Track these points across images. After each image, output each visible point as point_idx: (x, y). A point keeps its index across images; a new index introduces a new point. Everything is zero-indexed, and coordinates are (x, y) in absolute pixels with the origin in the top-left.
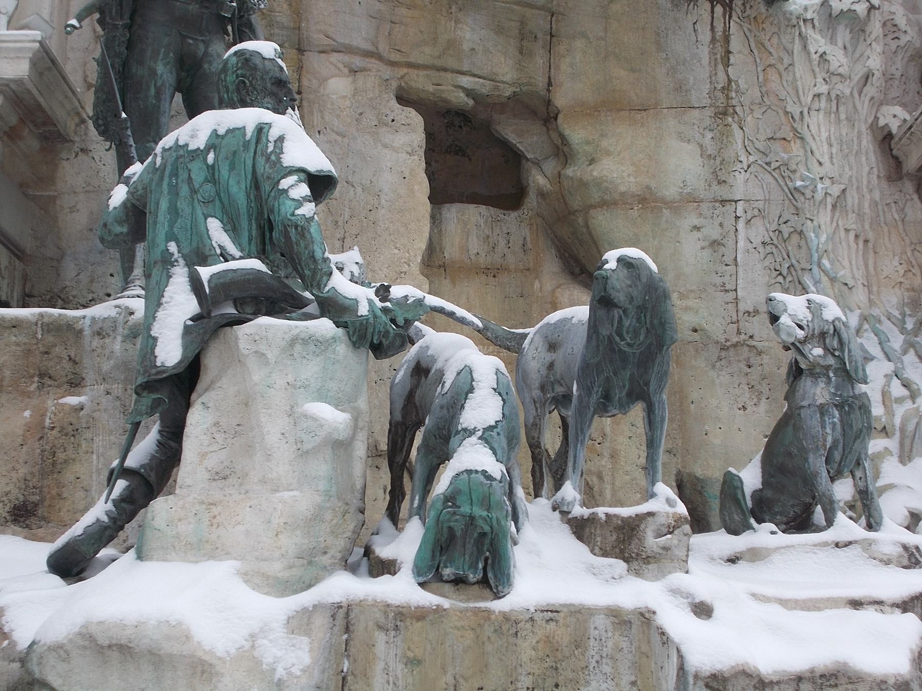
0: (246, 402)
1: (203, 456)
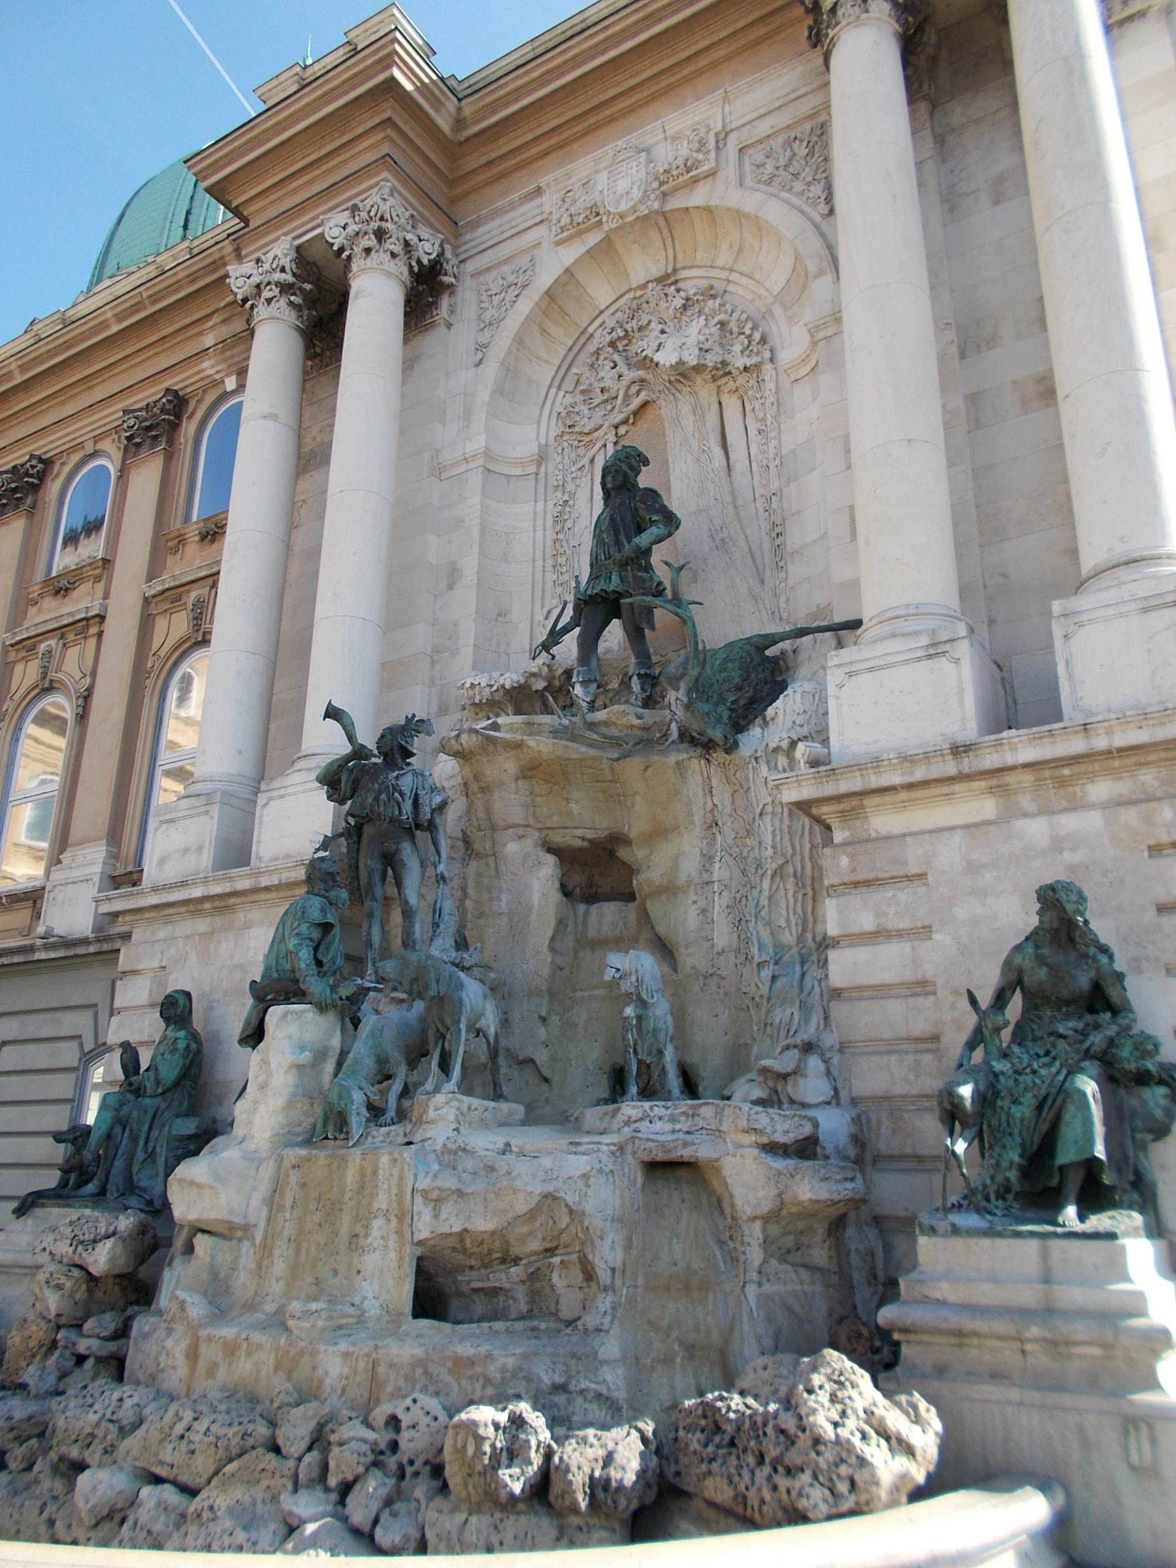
1: (257, 1077)
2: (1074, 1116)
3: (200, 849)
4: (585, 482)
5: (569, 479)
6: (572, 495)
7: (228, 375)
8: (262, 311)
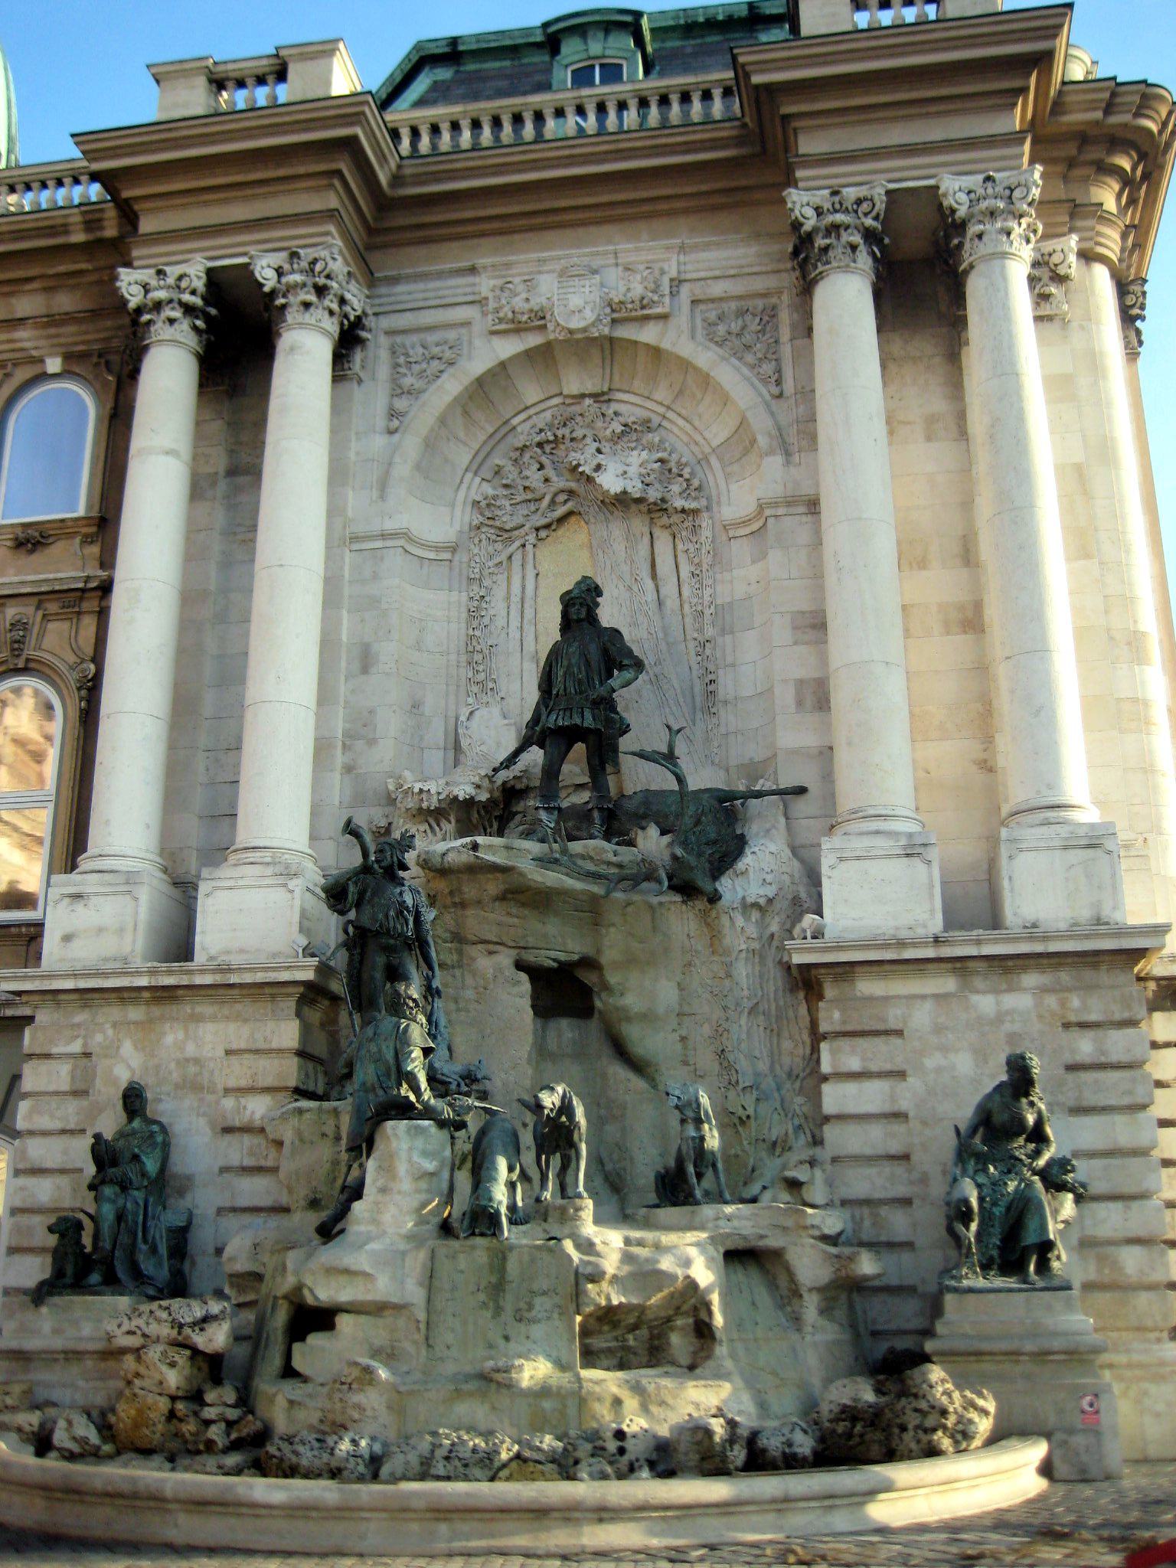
0: (391, 1156)
1: (374, 1181)
3: (121, 930)
4: (501, 579)
5: (486, 572)
6: (489, 590)
7: (51, 355)
8: (160, 331)
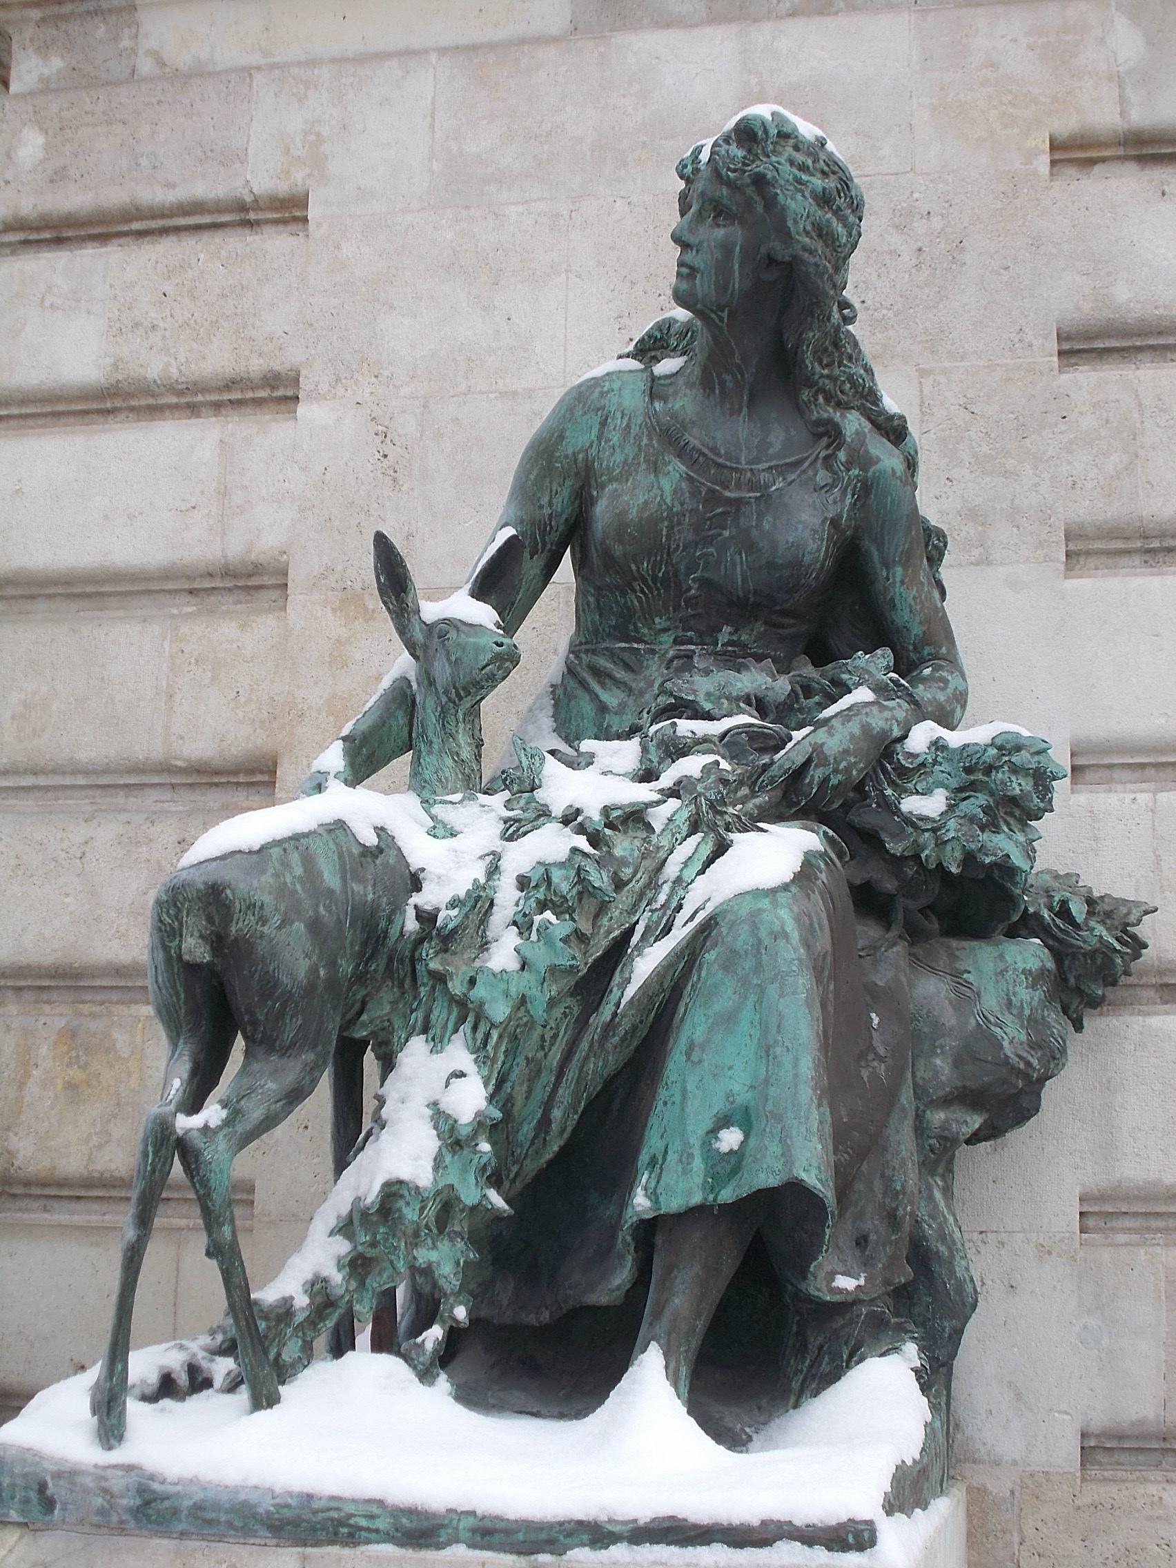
2: (729, 1019)
